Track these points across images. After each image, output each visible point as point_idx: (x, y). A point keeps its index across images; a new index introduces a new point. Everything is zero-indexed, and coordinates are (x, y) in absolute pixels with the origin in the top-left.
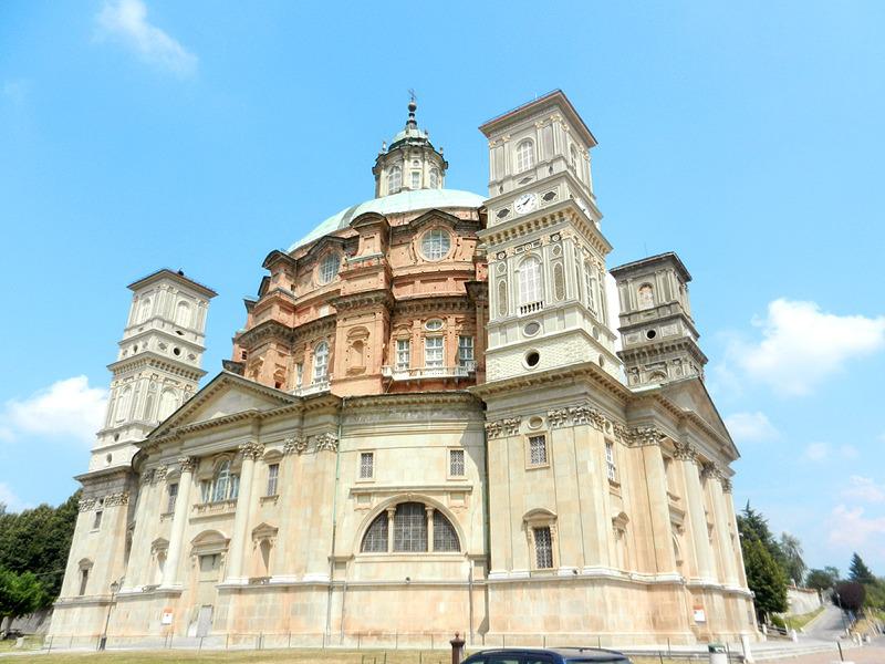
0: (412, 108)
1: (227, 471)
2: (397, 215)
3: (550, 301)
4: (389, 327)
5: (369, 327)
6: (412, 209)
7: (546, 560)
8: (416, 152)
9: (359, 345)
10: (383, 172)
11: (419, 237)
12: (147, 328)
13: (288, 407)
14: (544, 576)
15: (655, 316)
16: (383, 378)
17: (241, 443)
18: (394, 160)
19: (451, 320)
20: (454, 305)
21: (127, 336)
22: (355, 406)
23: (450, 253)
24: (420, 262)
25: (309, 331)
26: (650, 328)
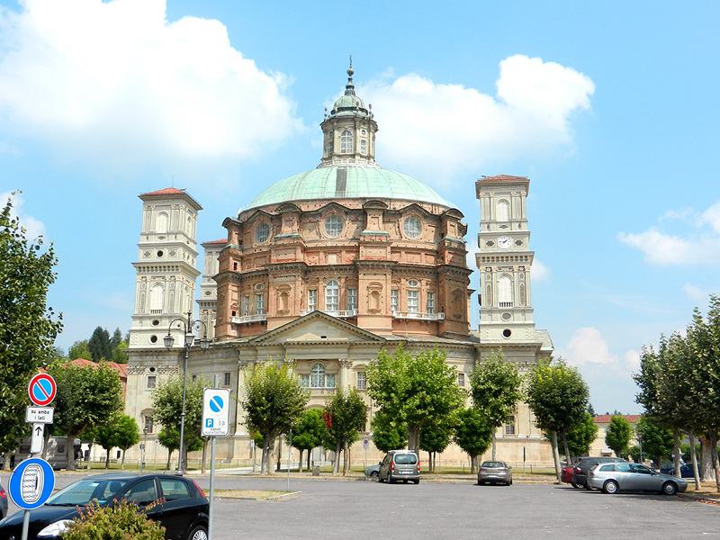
0: (350, 73)
1: (318, 370)
3: (517, 304)
5: (383, 283)
6: (394, 197)
8: (364, 124)
9: (375, 294)
10: (336, 132)
11: (402, 220)
12: (171, 240)
13: (376, 342)
14: (510, 438)
17: (341, 357)
18: (348, 125)
19: (424, 282)
21: (144, 241)
24: (404, 239)
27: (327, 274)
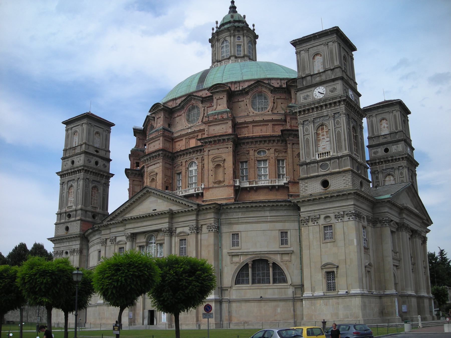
2: (235, 83)
4: (236, 153)
7: (331, 287)
8: (238, 31)
15: (389, 139)
16: (235, 186)
19: (272, 151)
20: (274, 141)
22: (227, 208)
23: (269, 108)
25: (184, 154)
26: (386, 146)
27: (187, 157)
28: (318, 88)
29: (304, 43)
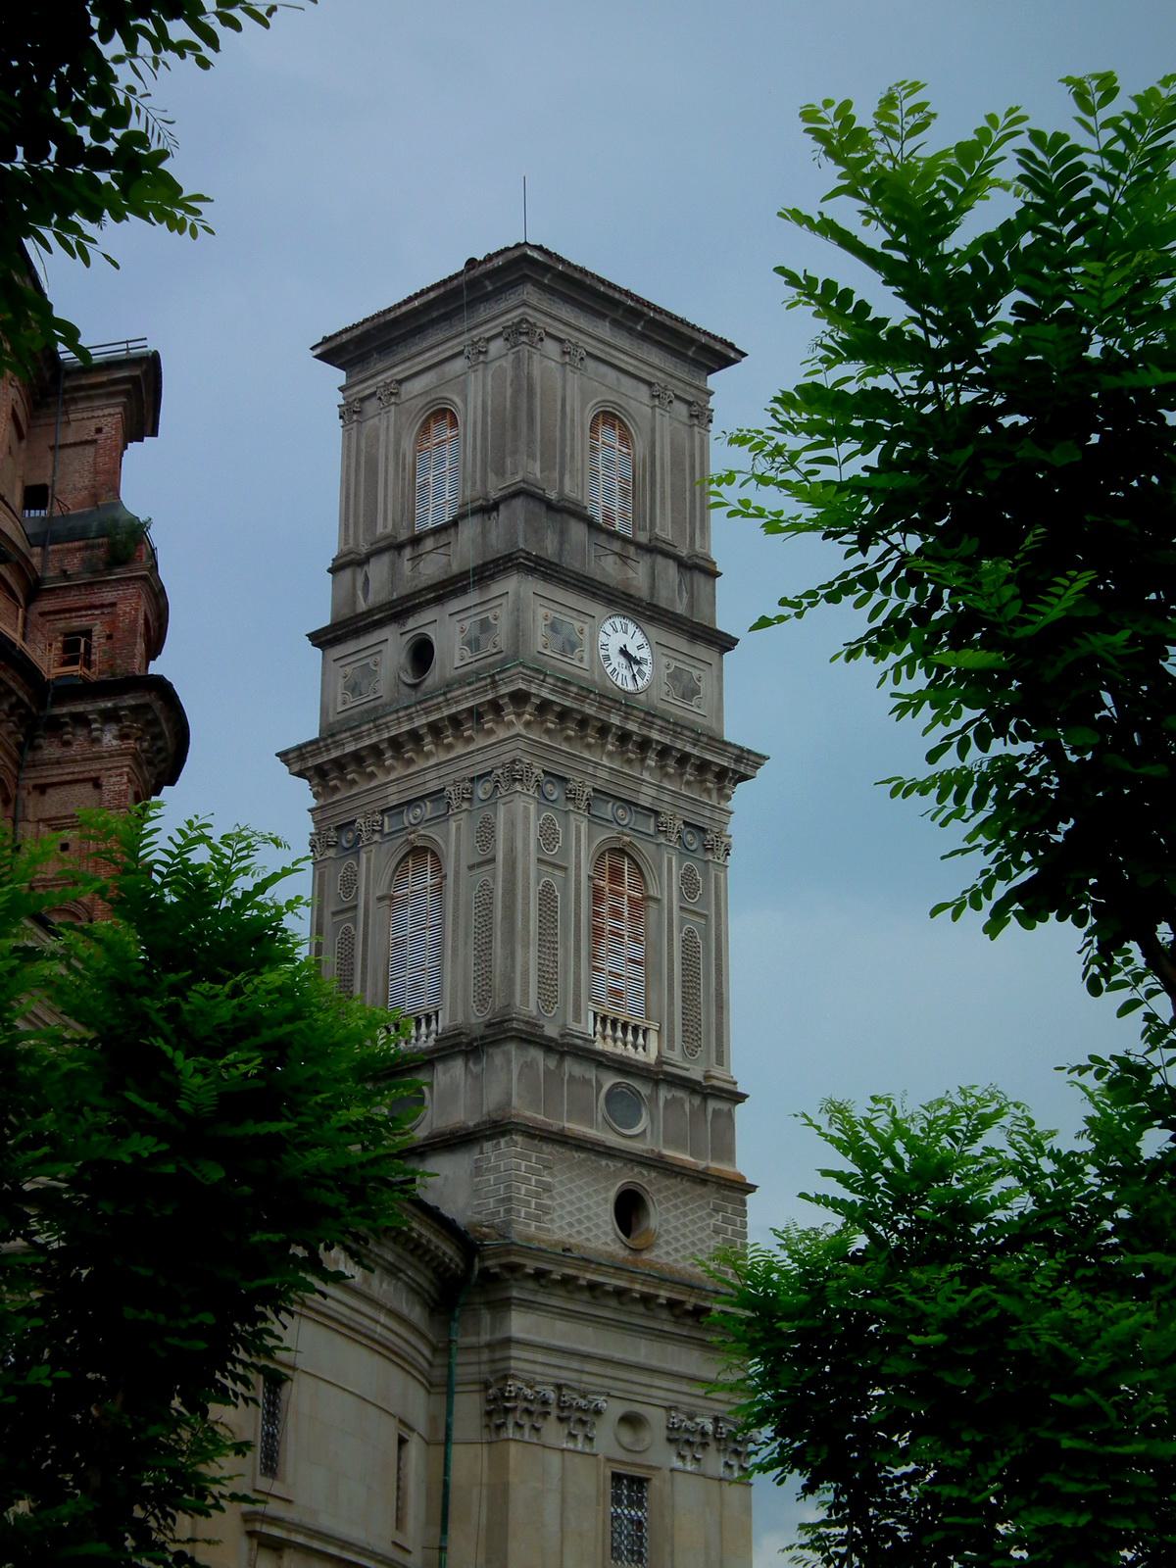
28: (618, 621)
29: (568, 300)
